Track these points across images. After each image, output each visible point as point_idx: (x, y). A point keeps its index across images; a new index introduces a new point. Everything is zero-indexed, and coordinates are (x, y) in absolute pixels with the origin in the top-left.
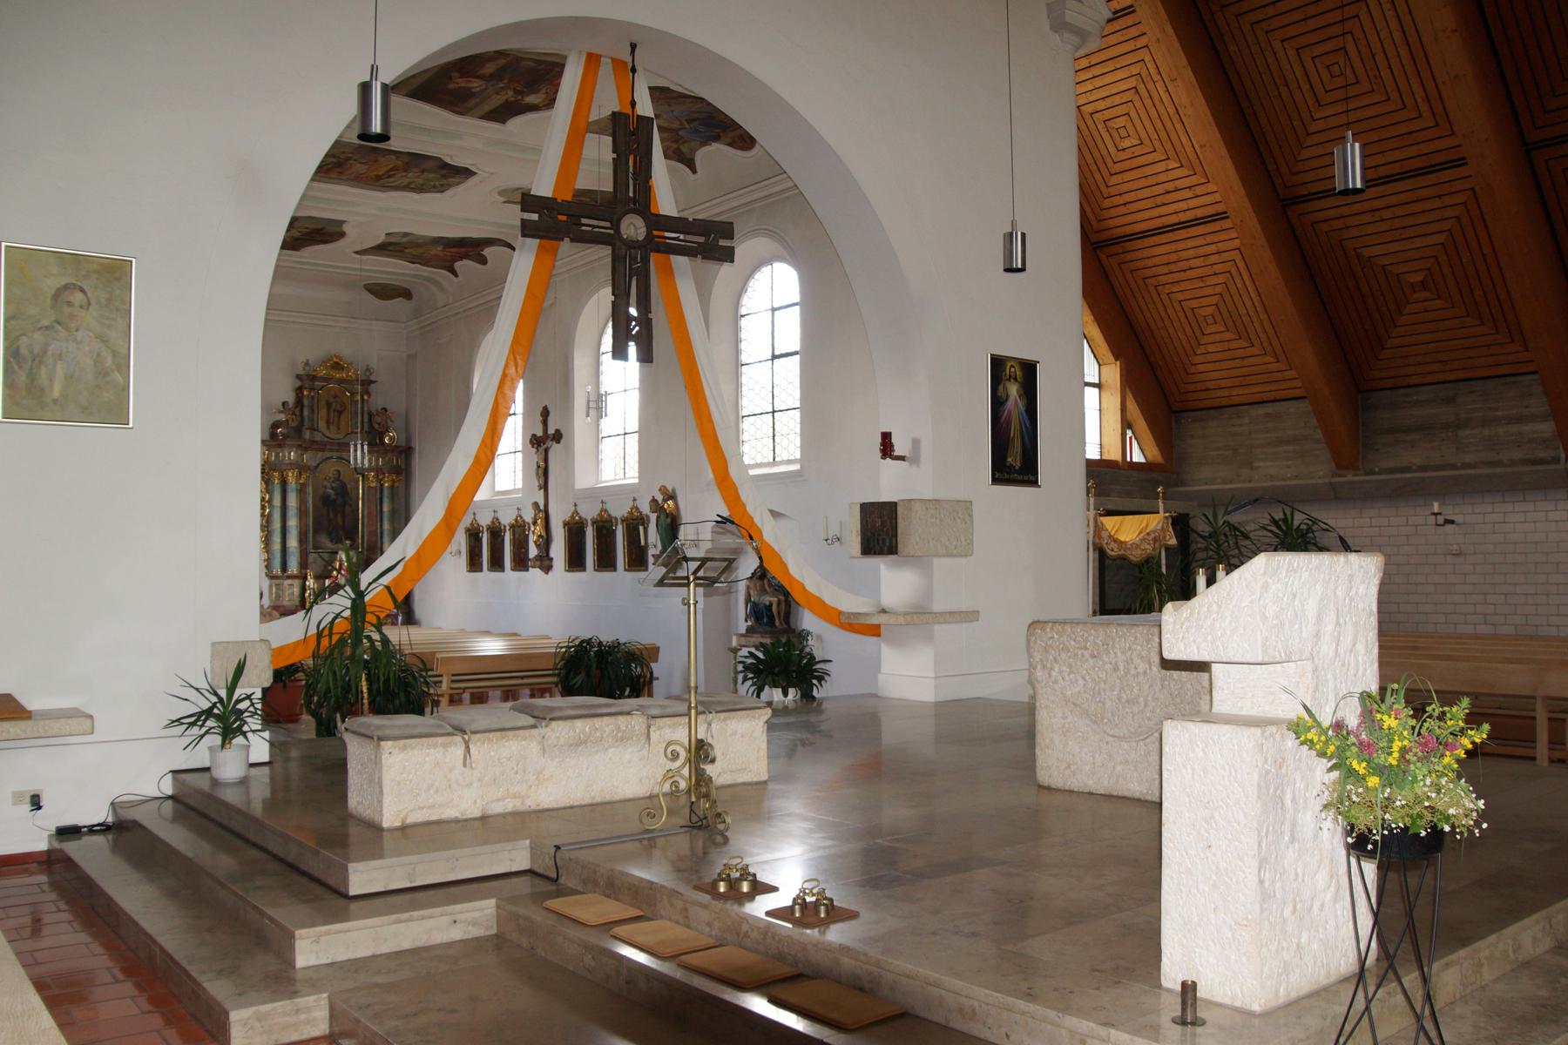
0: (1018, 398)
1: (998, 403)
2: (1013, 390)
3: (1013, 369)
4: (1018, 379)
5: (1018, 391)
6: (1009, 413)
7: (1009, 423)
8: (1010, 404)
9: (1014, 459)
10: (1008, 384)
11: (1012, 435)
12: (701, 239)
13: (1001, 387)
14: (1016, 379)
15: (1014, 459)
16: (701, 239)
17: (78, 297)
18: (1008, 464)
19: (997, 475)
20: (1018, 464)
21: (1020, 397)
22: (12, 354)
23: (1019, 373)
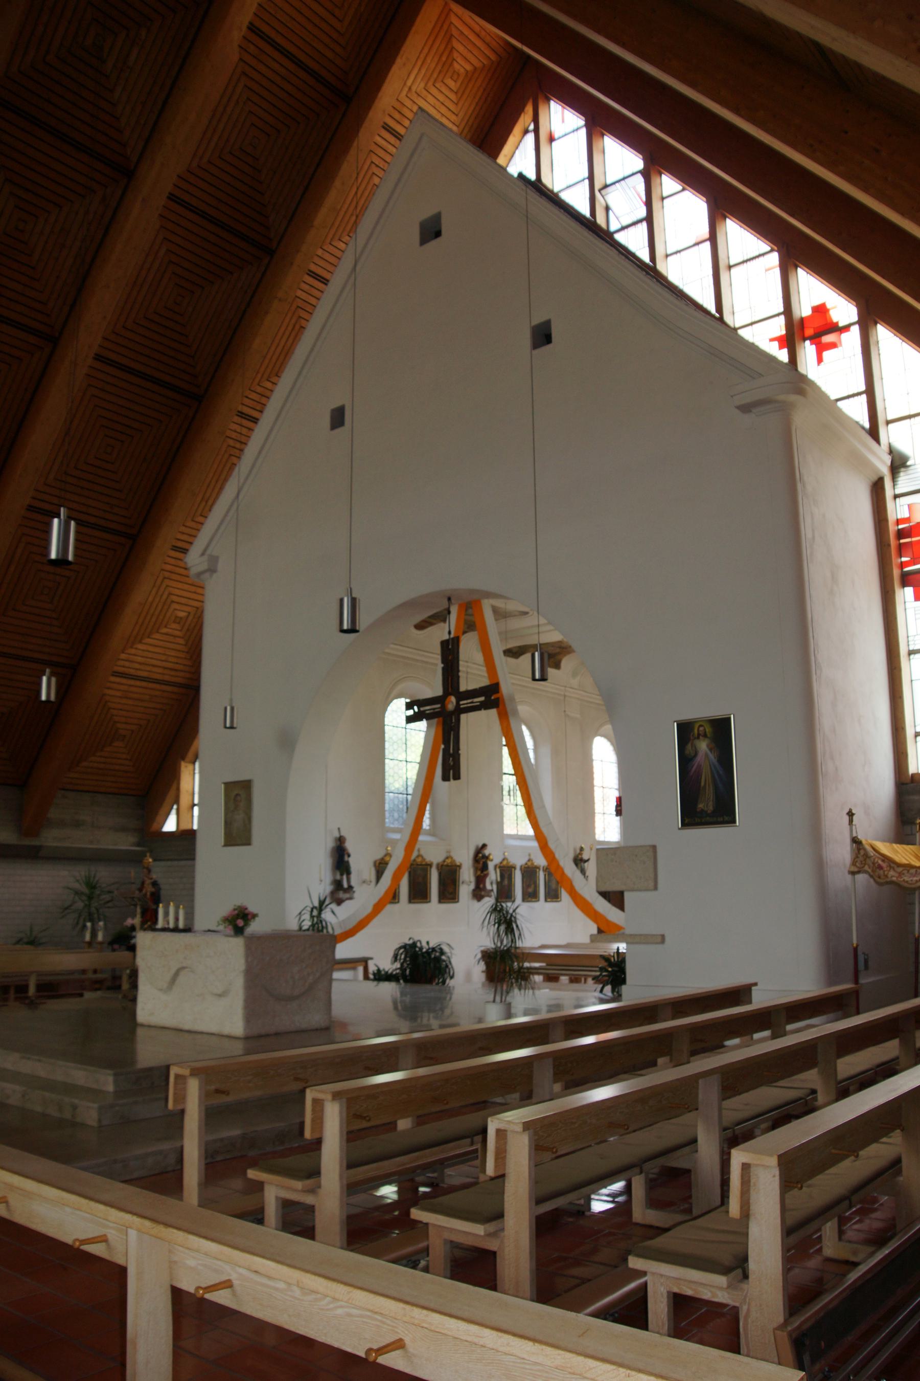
0: (709, 752)
1: (685, 761)
2: (703, 746)
3: (701, 729)
4: (709, 735)
5: (708, 746)
6: (699, 766)
7: (698, 774)
8: (700, 758)
9: (706, 804)
10: (697, 742)
11: (703, 784)
12: (482, 699)
13: (689, 747)
14: (705, 736)
15: (706, 804)
16: (482, 699)
17: (239, 798)
18: (698, 810)
19: (686, 821)
20: (711, 808)
21: (711, 750)
22: (226, 822)
23: (709, 730)
